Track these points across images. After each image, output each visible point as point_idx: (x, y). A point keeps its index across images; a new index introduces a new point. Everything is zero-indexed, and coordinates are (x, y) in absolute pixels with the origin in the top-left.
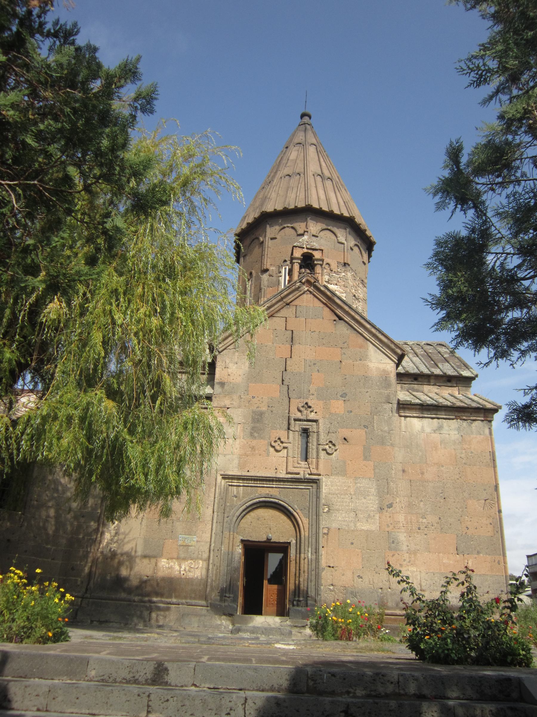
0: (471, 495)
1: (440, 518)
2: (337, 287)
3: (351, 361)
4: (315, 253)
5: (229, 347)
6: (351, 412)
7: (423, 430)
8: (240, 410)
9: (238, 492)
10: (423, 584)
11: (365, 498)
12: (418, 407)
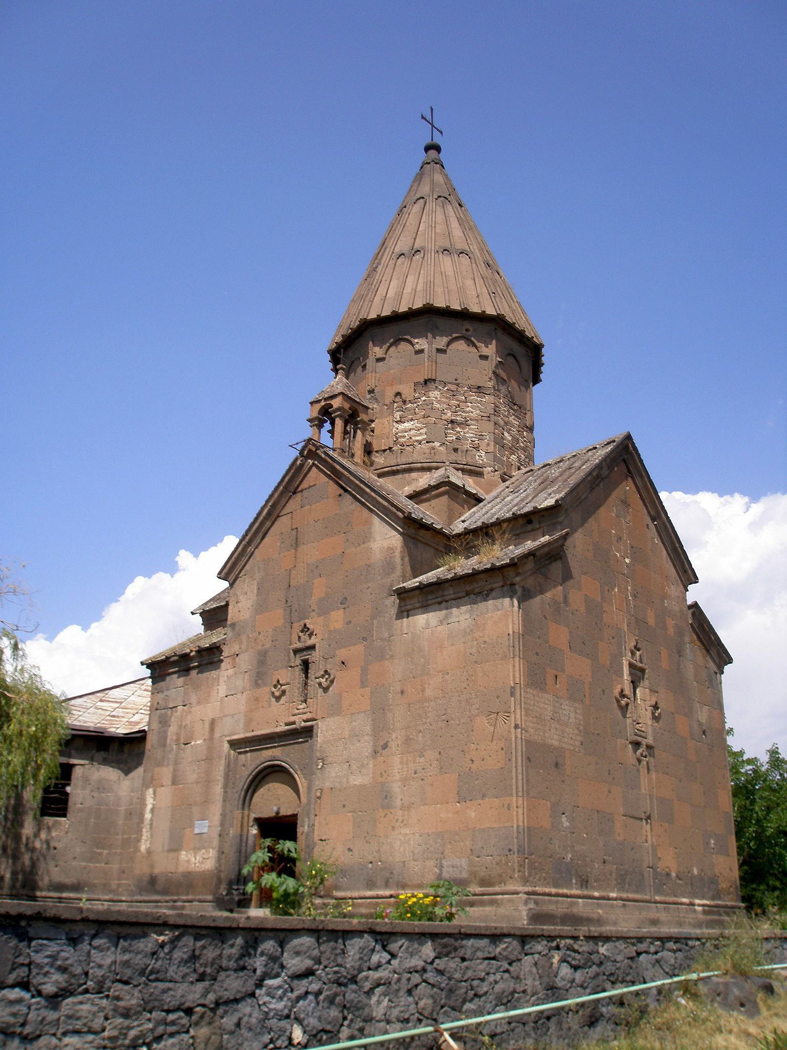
0: (481, 710)
1: (440, 752)
2: (412, 423)
3: (353, 549)
5: (240, 575)
6: (350, 622)
7: (427, 626)
8: (246, 654)
9: (246, 758)
10: (416, 852)
11: (359, 741)
12: (417, 592)
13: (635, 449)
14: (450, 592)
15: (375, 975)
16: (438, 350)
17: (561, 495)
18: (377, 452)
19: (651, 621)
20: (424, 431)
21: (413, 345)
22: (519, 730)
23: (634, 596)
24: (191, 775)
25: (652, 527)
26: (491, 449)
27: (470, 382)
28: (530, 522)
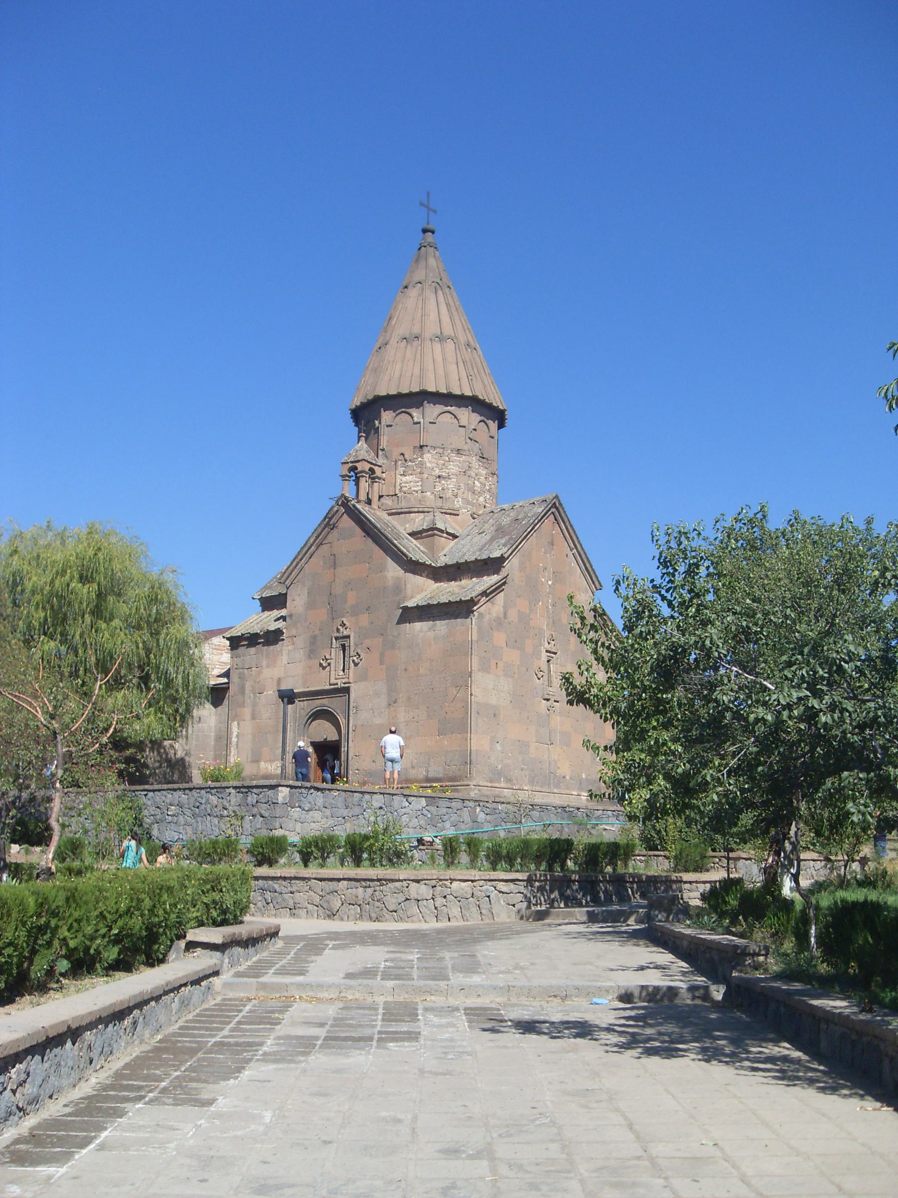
4: (357, 464)
13: (560, 504)
15: (403, 810)
16: (430, 423)
17: (505, 549)
18: (388, 496)
20: (420, 483)
21: (412, 418)
27: (453, 446)
28: (486, 564)
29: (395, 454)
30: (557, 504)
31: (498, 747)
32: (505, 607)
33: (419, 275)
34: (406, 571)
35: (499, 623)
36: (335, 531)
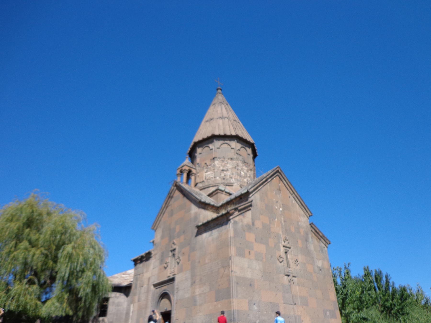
13: (281, 171)
14: (212, 225)
18: (200, 182)
19: (293, 230)
20: (213, 174)
21: (209, 147)
22: (233, 273)
23: (285, 221)
24: (143, 298)
25: (291, 197)
26: (236, 177)
28: (241, 198)
29: (203, 164)
30: (280, 171)
31: (255, 307)
32: (252, 219)
33: (215, 101)
34: (199, 207)
35: (250, 228)
36: (173, 200)
